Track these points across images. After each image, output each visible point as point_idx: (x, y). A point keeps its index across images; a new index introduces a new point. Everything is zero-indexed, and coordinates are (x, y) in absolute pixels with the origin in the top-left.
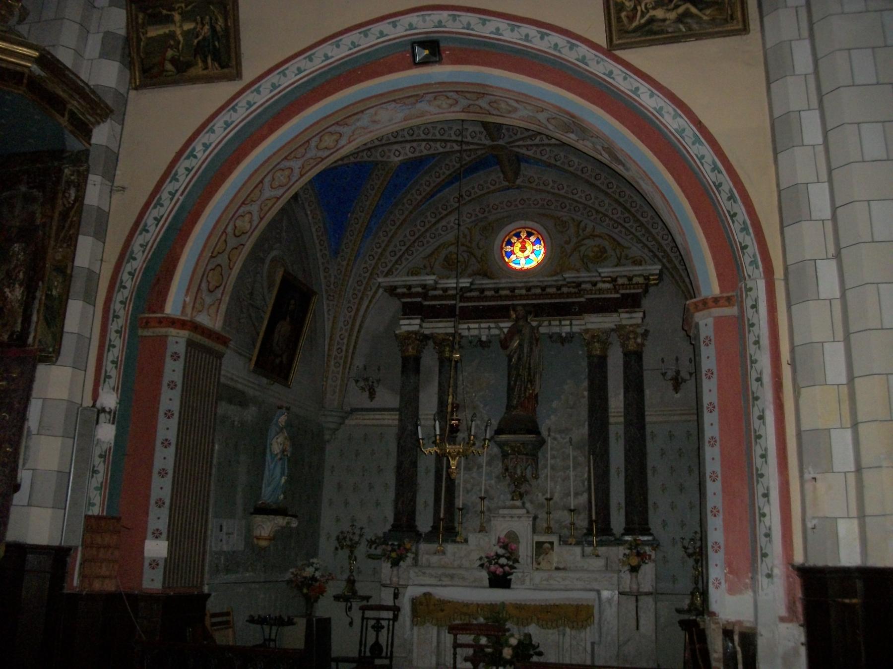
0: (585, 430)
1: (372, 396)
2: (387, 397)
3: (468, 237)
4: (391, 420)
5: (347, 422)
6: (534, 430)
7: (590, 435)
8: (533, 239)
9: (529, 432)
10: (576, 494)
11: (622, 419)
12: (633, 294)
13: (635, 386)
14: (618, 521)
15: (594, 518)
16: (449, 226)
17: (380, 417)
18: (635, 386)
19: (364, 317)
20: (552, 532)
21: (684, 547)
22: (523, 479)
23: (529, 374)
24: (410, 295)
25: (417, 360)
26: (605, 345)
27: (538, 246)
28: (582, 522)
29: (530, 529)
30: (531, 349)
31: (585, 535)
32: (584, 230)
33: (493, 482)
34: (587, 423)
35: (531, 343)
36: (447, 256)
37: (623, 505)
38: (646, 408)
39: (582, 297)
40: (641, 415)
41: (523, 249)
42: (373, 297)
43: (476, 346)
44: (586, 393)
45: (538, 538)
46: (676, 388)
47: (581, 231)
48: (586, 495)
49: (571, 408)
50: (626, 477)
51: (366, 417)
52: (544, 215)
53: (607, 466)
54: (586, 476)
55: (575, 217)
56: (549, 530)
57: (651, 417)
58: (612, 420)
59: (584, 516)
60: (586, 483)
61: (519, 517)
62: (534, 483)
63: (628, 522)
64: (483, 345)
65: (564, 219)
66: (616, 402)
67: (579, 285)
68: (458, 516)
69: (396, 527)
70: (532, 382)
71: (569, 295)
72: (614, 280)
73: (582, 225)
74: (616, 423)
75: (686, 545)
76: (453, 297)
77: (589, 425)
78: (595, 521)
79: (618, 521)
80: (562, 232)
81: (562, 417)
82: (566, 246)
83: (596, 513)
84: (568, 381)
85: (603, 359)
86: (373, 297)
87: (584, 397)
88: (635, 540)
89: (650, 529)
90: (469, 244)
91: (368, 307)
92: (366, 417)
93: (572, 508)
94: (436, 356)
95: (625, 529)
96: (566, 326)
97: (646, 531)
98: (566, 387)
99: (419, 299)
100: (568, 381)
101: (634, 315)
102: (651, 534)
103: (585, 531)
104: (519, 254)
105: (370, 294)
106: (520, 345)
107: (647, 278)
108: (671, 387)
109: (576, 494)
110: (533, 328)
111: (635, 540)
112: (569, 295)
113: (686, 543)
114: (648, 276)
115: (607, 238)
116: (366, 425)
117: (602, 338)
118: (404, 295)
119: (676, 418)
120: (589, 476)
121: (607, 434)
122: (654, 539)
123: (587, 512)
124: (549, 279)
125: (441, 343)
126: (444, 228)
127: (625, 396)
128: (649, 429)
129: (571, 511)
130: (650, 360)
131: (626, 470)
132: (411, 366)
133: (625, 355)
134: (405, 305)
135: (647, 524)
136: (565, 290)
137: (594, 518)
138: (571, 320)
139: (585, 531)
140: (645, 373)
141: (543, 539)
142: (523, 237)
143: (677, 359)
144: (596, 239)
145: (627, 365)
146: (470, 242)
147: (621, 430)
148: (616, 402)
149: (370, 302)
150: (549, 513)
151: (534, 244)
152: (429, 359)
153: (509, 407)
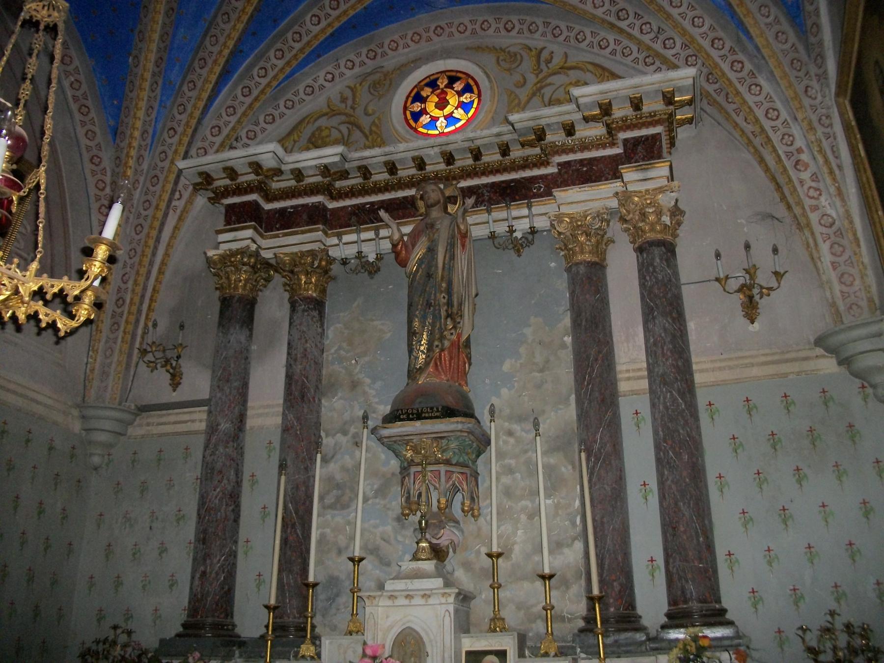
0: (570, 412)
1: (175, 381)
2: (198, 381)
3: (350, 102)
4: (197, 420)
5: (130, 431)
6: (459, 409)
7: (580, 417)
8: (459, 86)
9: (449, 412)
10: (557, 546)
11: (644, 384)
12: (647, 138)
13: (663, 304)
14: (651, 599)
15: (596, 591)
16: (316, 85)
17: (186, 417)
18: (663, 304)
19: (169, 245)
20: (503, 629)
21: (810, 650)
22: (444, 517)
23: (449, 304)
24: (240, 190)
25: (250, 305)
26: (602, 242)
27: (468, 95)
28: (572, 604)
29: (449, 623)
30: (453, 257)
31: (582, 631)
32: (548, 61)
33: (389, 529)
34: (573, 397)
35: (451, 246)
36: (313, 134)
37: (660, 561)
38: (694, 359)
39: (546, 164)
40: (685, 371)
41: (442, 104)
42: (185, 211)
43: (355, 271)
44: (568, 340)
45: (470, 644)
46: (751, 310)
47: (543, 66)
48: (579, 545)
49: (541, 371)
50: (662, 497)
51: (164, 420)
52: (479, 48)
53: (620, 480)
54: (577, 503)
55: (531, 43)
56: (496, 625)
57: (704, 371)
58: (623, 386)
59: (577, 588)
60: (578, 520)
61: (425, 596)
62: (469, 525)
63: (673, 602)
64: (371, 269)
65: (512, 49)
66: (630, 352)
67: (540, 134)
68: (318, 600)
69: (191, 628)
70: (454, 316)
71: (526, 164)
72: (606, 109)
73: (545, 55)
74: (634, 393)
75: (814, 644)
76: (313, 190)
77: (579, 402)
78: (600, 599)
79: (651, 599)
80: (509, 70)
81: (520, 378)
82: (517, 91)
83: (601, 581)
84: (533, 320)
85: (597, 268)
86: (185, 211)
87: (563, 346)
88: (695, 639)
89: (724, 611)
90: (351, 112)
91: (176, 228)
92: (164, 420)
93: (547, 571)
94: (287, 295)
95: (669, 615)
96: (520, 218)
97: (718, 617)
98: (528, 331)
99: (253, 197)
100: (533, 320)
101: (651, 174)
102: (730, 623)
103: (581, 624)
104: (436, 113)
105: (180, 204)
106: (431, 250)
107: (668, 99)
108: (739, 312)
109: (557, 546)
110: (454, 217)
111: (695, 639)
112: (526, 164)
113: (812, 639)
114: (673, 94)
115: (590, 67)
116: (161, 435)
117: (594, 232)
118: (227, 192)
119: (755, 372)
120: (583, 504)
121: (616, 417)
122: (738, 636)
123: (583, 582)
124: (486, 132)
125: (289, 269)
126: (309, 90)
127: (647, 330)
128: (702, 401)
129: (543, 577)
130: (692, 261)
131: (661, 483)
132: (237, 311)
133: (640, 250)
134: (230, 208)
135: (719, 601)
136: (517, 153)
137: (596, 591)
138: (529, 207)
139: (581, 624)
140: (684, 289)
141: (481, 644)
142: (442, 86)
143: (747, 247)
144: (571, 72)
145: (645, 270)
146: (353, 108)
147: (644, 405)
148: (630, 352)
149: (181, 219)
150: (496, 587)
151: (460, 94)
152: (273, 305)
153: (413, 373)
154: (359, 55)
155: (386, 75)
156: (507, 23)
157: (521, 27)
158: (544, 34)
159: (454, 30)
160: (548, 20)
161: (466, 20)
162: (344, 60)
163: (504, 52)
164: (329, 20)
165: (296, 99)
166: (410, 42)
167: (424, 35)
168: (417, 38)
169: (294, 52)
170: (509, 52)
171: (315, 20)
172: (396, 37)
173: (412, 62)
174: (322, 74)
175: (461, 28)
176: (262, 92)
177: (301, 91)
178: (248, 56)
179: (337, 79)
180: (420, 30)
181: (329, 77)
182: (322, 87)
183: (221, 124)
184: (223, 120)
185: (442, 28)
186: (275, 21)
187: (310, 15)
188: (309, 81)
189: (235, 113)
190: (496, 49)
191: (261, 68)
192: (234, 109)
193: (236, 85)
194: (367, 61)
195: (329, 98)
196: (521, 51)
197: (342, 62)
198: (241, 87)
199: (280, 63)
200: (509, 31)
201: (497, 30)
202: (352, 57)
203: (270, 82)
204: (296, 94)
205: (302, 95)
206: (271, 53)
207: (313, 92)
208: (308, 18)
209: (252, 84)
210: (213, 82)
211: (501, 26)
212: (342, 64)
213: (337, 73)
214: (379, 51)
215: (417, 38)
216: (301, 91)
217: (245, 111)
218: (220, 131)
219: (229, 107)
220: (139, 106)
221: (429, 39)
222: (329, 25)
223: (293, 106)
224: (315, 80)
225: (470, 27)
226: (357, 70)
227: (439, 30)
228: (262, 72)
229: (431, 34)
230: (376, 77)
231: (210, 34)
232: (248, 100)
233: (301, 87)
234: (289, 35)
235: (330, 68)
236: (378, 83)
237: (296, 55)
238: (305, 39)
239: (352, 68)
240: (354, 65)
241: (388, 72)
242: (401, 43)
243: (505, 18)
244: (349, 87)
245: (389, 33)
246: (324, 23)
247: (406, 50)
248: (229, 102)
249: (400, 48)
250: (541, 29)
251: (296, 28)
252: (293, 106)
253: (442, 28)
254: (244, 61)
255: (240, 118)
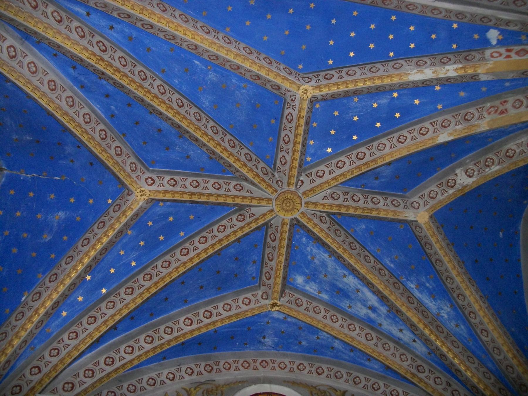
16: (158, 380)
65: (322, 388)
154: (198, 366)
155: (217, 387)
156: (318, 368)
157: (329, 373)
158: (347, 381)
159: (276, 365)
160: (350, 372)
161: (286, 361)
162: (186, 367)
163: (316, 389)
164: (199, 325)
165: (139, 386)
166: (240, 367)
167: (252, 365)
168: (246, 365)
169: (163, 341)
170: (319, 390)
171: (188, 322)
172: (230, 361)
173: (240, 382)
174: (165, 372)
175: (282, 366)
176: (123, 366)
177: (145, 381)
178: (121, 334)
179: (177, 379)
180: (250, 360)
181: (171, 376)
182: (163, 383)
183: (76, 382)
184: (78, 379)
185: (266, 362)
186: (152, 314)
187: (184, 318)
188: (153, 375)
189: (93, 376)
190: (308, 386)
191: (129, 347)
192: (93, 373)
193: (100, 354)
194: (204, 372)
195: (167, 393)
196: (329, 391)
197: (184, 368)
198: (105, 357)
199: (148, 347)
200: (319, 374)
201: (310, 372)
202: (193, 366)
203: (133, 360)
204: (140, 381)
205: (144, 384)
206: (142, 337)
207: (154, 384)
208: (182, 319)
209: (117, 357)
210: (95, 339)
211: (314, 370)
212: (183, 370)
213: (177, 375)
214: (215, 367)
215: (247, 365)
216: (145, 381)
217: (102, 378)
218: (72, 388)
219: (89, 370)
220: (19, 335)
221: (256, 368)
222: (199, 329)
223: (135, 391)
224: (158, 375)
225: (289, 366)
226: (194, 377)
227: (264, 364)
228: (129, 350)
229: (258, 364)
230: (209, 387)
231: (108, 300)
232: (109, 369)
233: (145, 378)
234: (162, 328)
235: (172, 370)
236: (211, 391)
237: (163, 344)
238: (175, 334)
239: (191, 375)
240: (193, 372)
241: (219, 385)
242: (234, 366)
243: (317, 365)
244: (185, 389)
245: (225, 357)
246: (195, 326)
247: (237, 372)
248: (90, 366)
249: (232, 369)
250: (345, 376)
251: (170, 324)
252: (135, 391)
253: (266, 362)
254: (113, 338)
255: (95, 382)
